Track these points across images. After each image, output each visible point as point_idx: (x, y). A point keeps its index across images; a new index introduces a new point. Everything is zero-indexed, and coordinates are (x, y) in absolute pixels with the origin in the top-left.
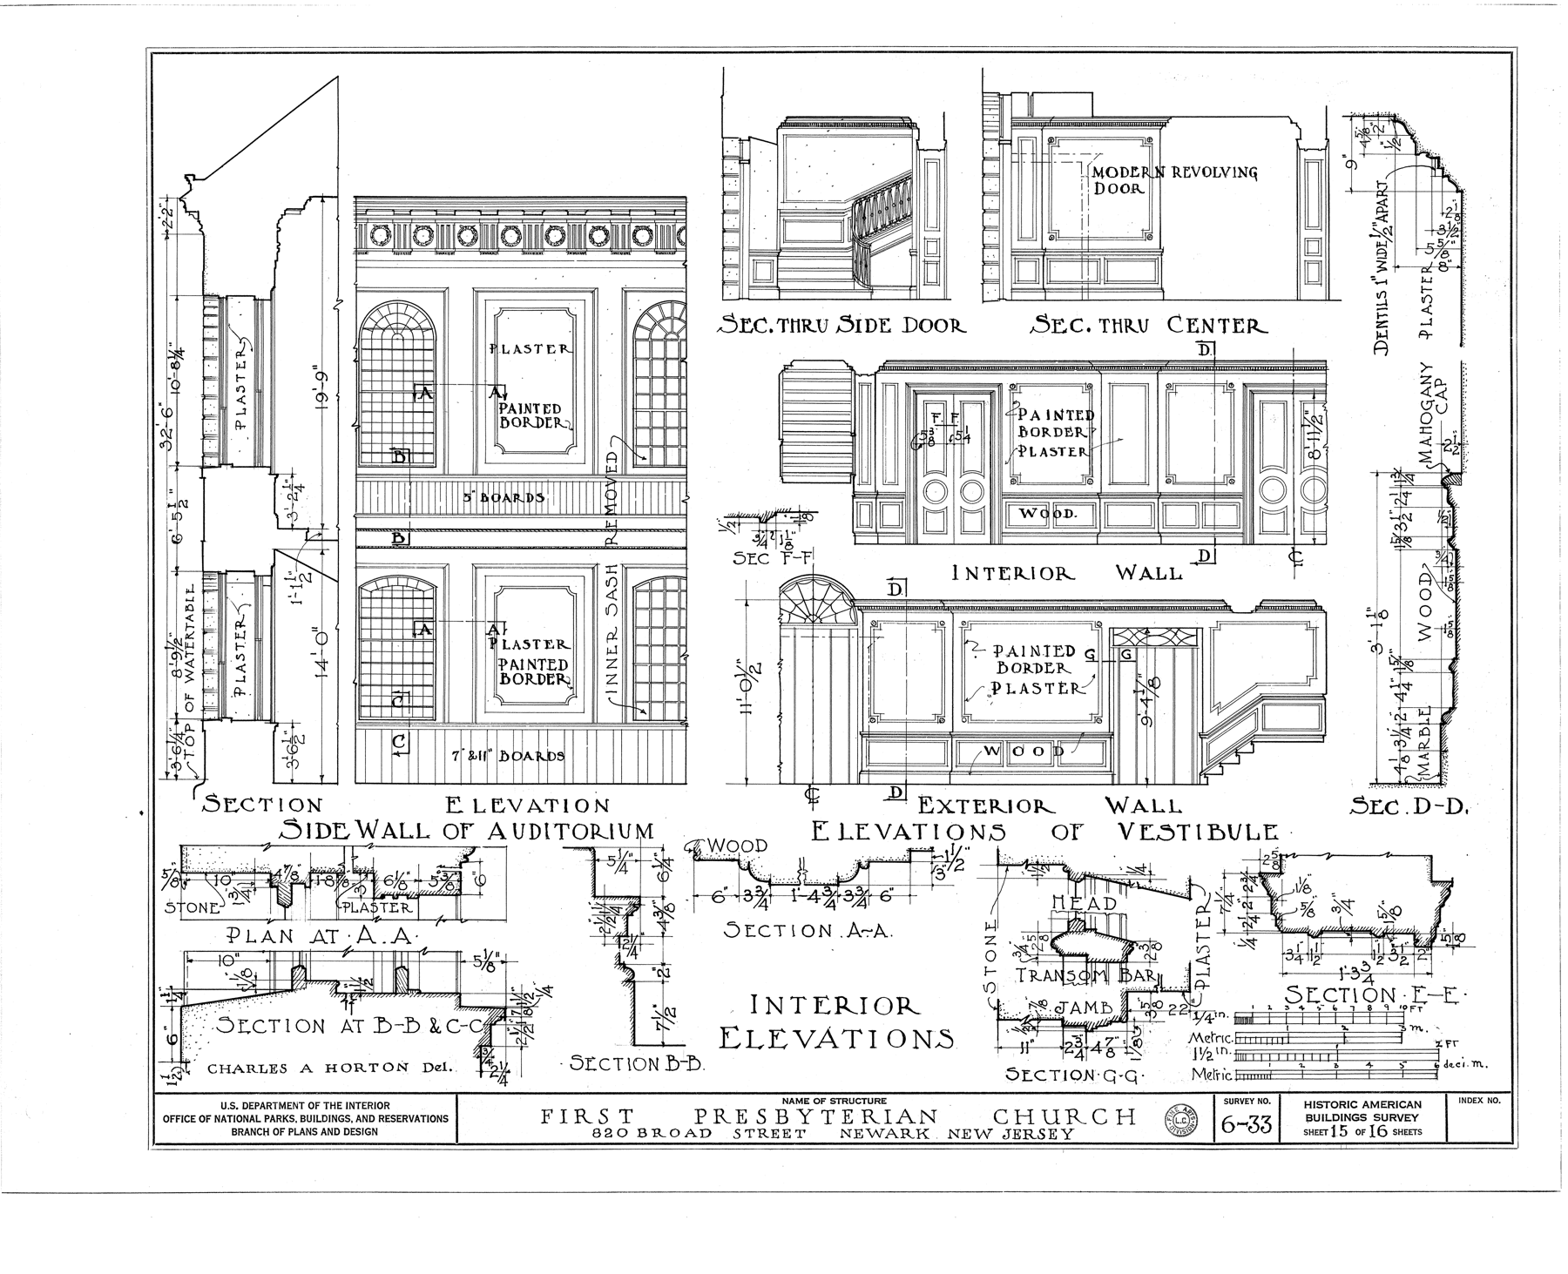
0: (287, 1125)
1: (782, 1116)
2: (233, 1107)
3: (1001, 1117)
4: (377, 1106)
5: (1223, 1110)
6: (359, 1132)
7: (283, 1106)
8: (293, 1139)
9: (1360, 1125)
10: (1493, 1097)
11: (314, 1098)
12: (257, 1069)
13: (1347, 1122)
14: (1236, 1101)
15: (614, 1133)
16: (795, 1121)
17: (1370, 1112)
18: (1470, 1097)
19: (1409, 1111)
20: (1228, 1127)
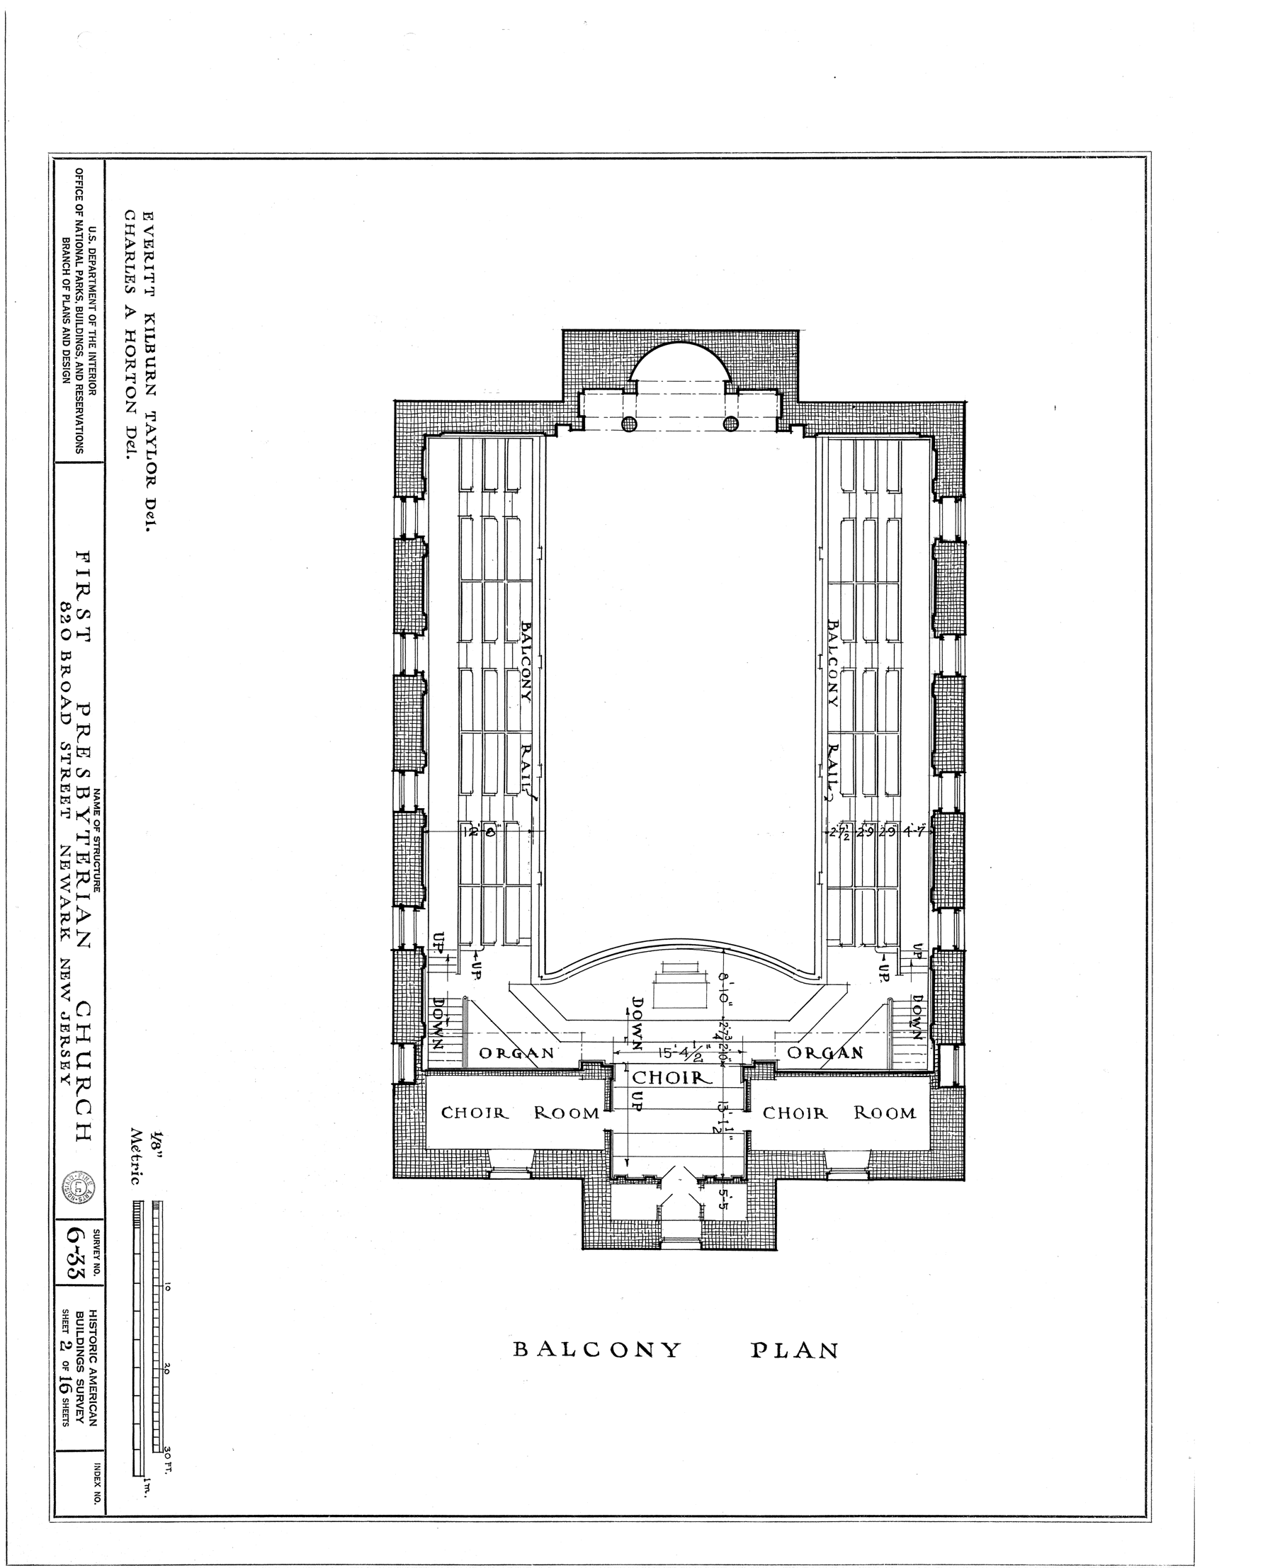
0: (73, 293)
1: (84, 793)
2: (92, 239)
3: (84, 1009)
5: (88, 1227)
6: (66, 365)
7: (92, 288)
8: (59, 299)
9: (73, 1366)
10: (101, 1498)
11: (100, 321)
12: (130, 263)
13: (74, 1350)
14: (97, 1242)
15: (66, 625)
16: (79, 805)
17: (85, 1376)
18: (101, 1475)
19: (87, 1414)
20: (73, 1235)
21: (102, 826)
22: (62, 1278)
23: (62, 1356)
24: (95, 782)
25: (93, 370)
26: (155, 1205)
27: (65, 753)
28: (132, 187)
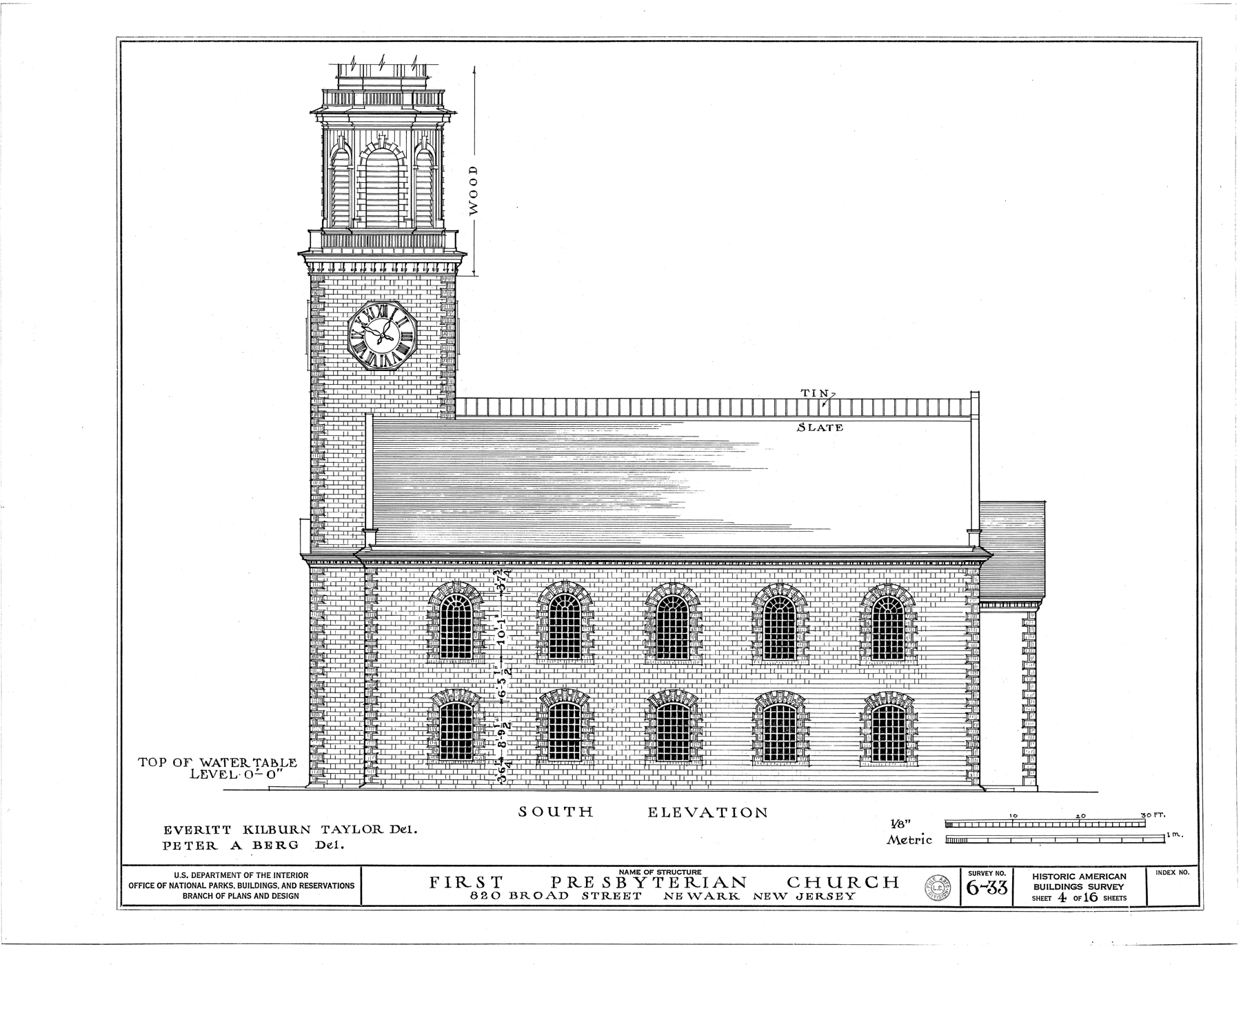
0: (227, 891)
1: (622, 882)
2: (184, 876)
4: (298, 875)
6: (284, 896)
7: (223, 875)
9: (1077, 893)
11: (249, 869)
14: (978, 873)
15: (489, 895)
17: (1085, 883)
18: (1165, 870)
19: (1117, 881)
20: (973, 890)
22: (1005, 900)
24: (613, 874)
26: (949, 825)
27: (591, 897)
28: (144, 843)
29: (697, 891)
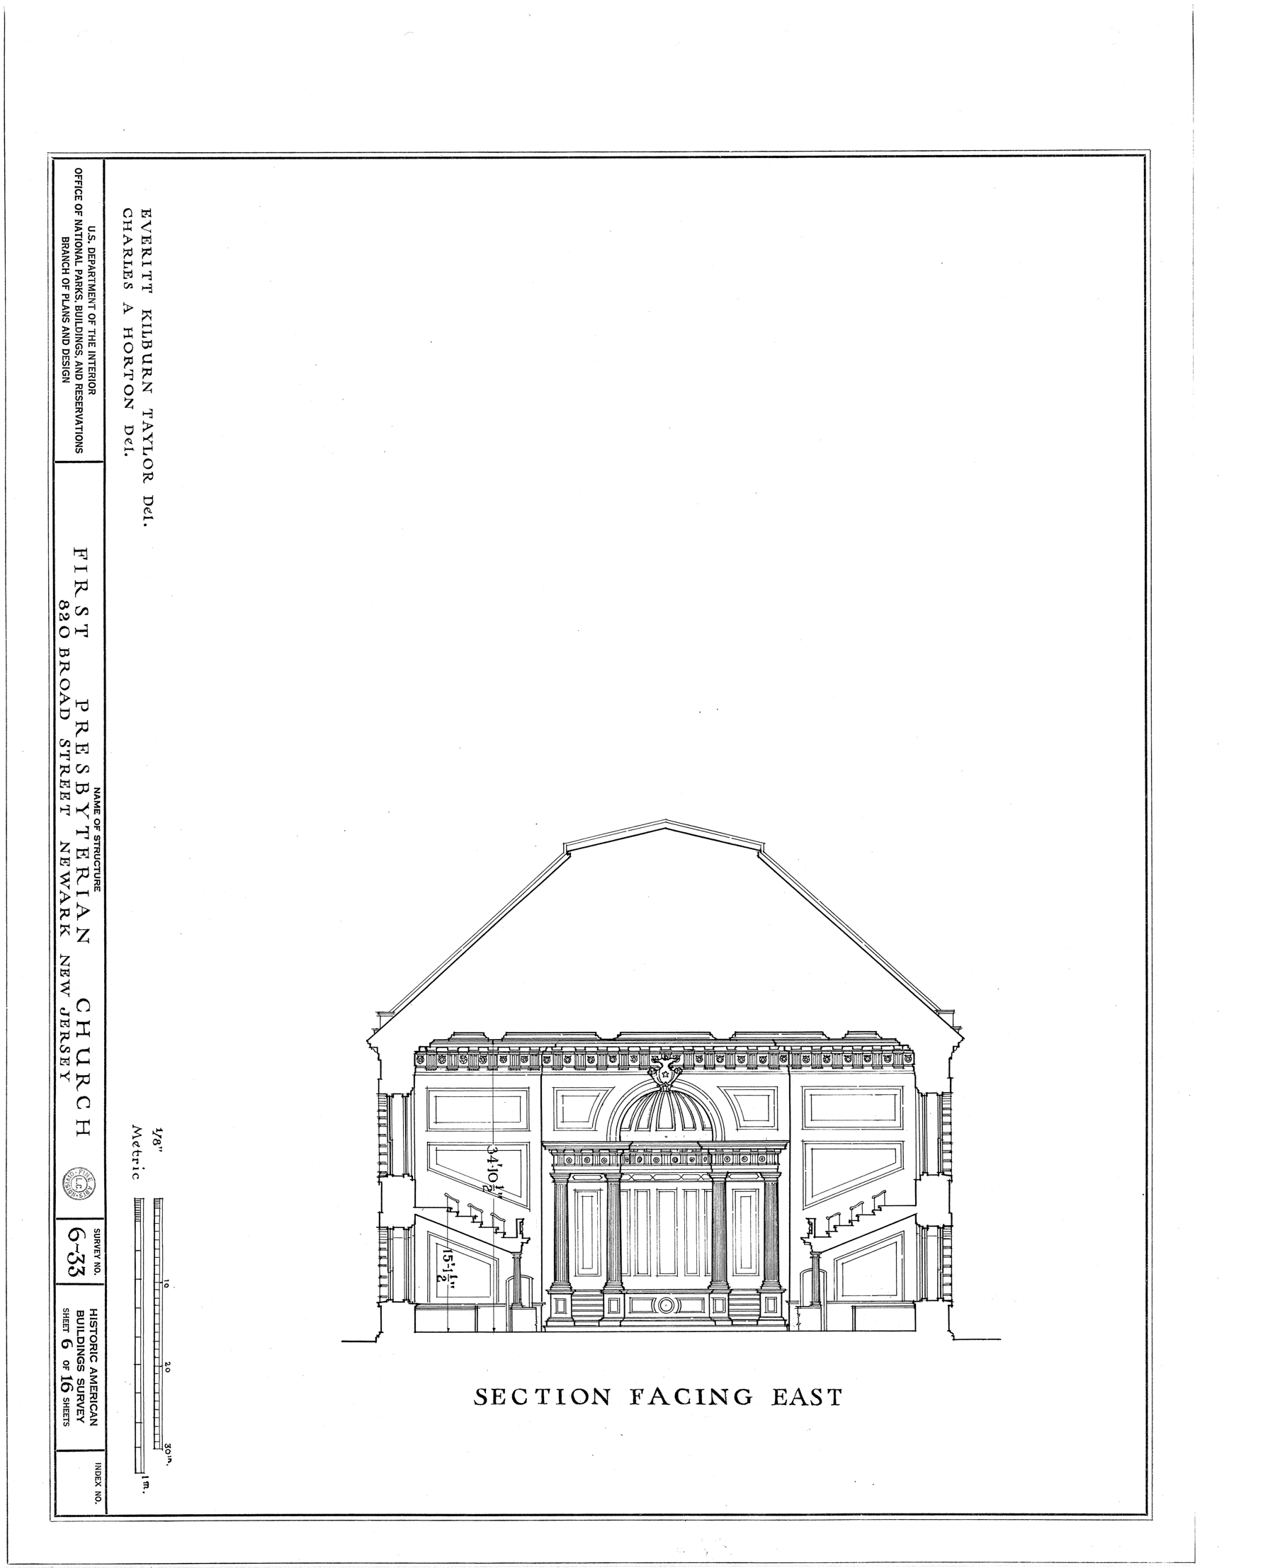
0: (72, 292)
1: (83, 788)
2: (91, 238)
3: (83, 1005)
6: (66, 364)
7: (92, 287)
11: (99, 320)
12: (128, 259)
14: (98, 1241)
15: (64, 623)
16: (77, 801)
17: (86, 1375)
18: (101, 1474)
19: (88, 1414)
20: (74, 1235)
21: (102, 825)
22: (63, 1276)
23: (62, 1355)
25: (92, 369)
26: (157, 1202)
29: (72, 883)
